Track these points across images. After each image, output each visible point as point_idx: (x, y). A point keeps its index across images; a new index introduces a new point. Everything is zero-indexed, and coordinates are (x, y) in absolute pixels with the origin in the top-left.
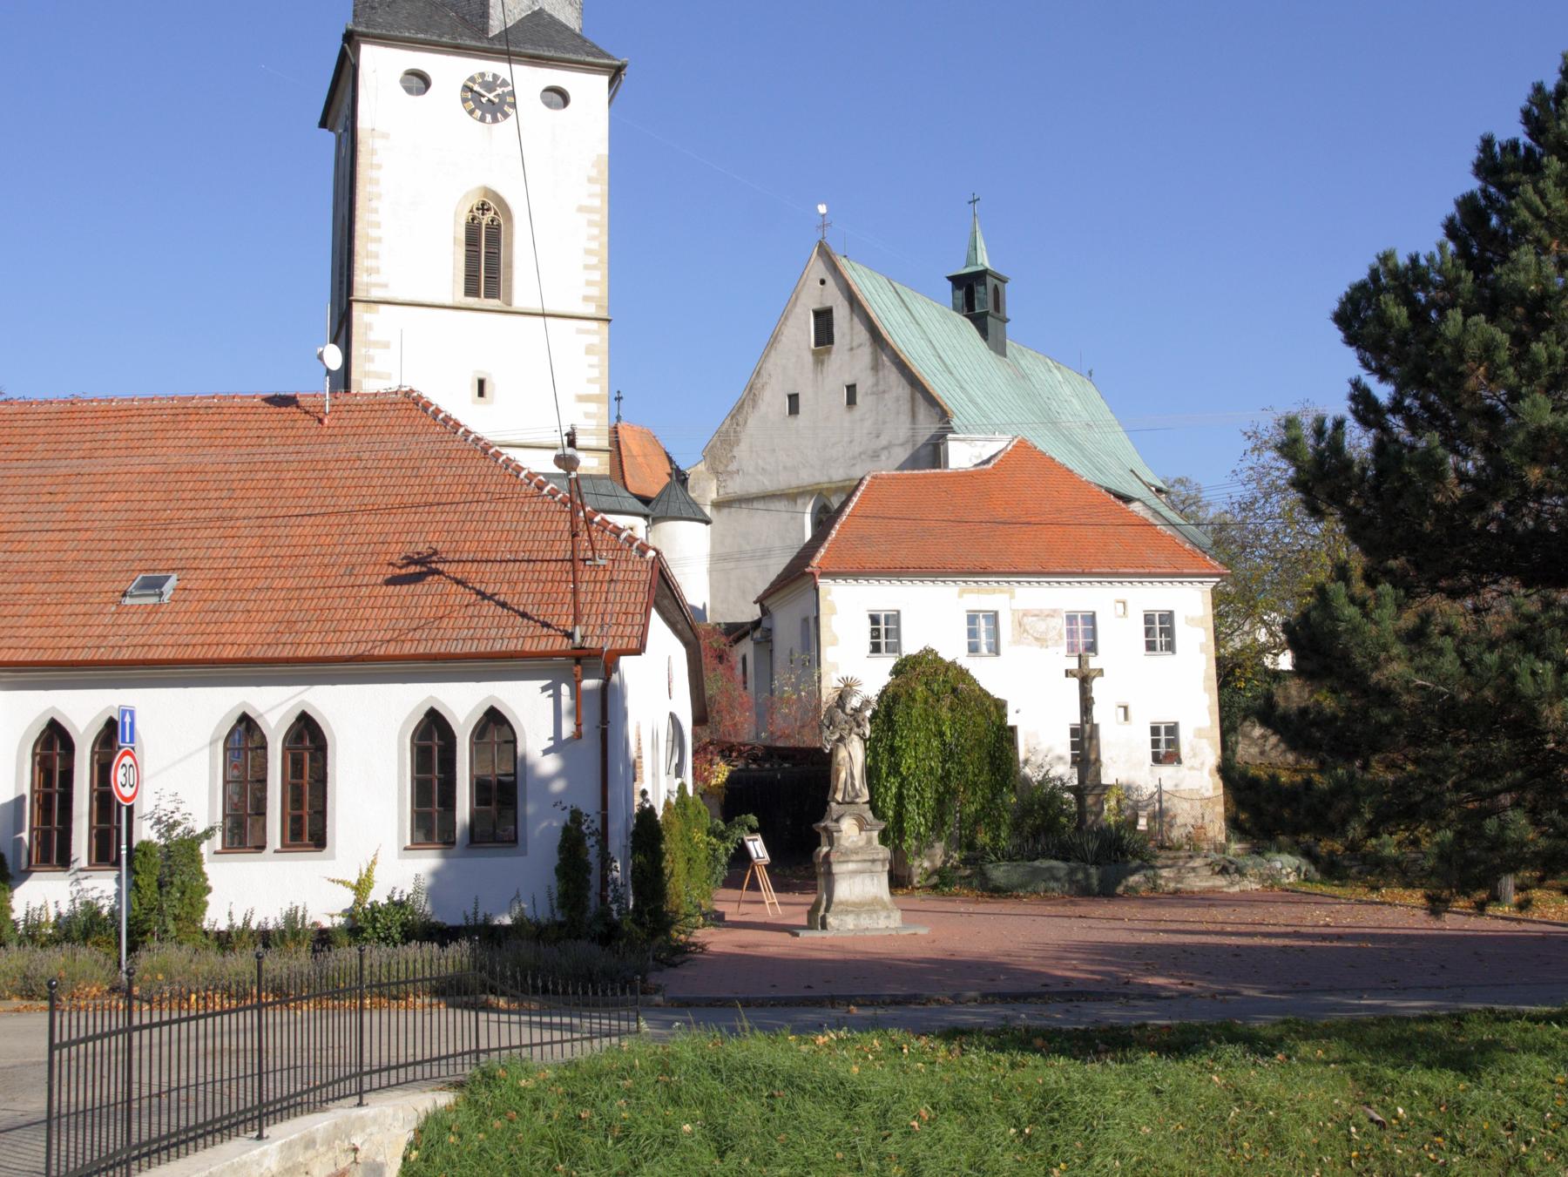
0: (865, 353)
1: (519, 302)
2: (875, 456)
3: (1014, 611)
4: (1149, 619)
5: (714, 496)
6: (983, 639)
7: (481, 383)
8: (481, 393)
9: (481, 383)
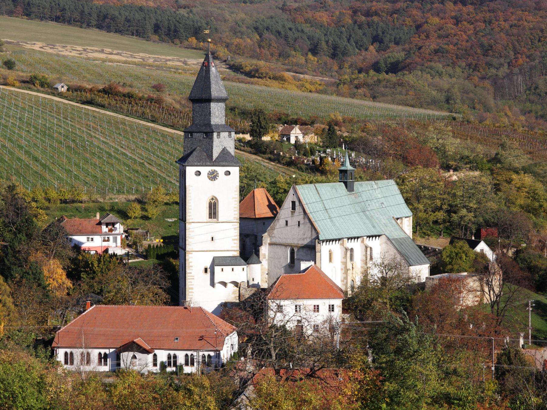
1: (220, 219)
2: (303, 240)
4: (329, 306)
5: (269, 242)
6: (298, 309)
7: (212, 238)
9: (212, 238)
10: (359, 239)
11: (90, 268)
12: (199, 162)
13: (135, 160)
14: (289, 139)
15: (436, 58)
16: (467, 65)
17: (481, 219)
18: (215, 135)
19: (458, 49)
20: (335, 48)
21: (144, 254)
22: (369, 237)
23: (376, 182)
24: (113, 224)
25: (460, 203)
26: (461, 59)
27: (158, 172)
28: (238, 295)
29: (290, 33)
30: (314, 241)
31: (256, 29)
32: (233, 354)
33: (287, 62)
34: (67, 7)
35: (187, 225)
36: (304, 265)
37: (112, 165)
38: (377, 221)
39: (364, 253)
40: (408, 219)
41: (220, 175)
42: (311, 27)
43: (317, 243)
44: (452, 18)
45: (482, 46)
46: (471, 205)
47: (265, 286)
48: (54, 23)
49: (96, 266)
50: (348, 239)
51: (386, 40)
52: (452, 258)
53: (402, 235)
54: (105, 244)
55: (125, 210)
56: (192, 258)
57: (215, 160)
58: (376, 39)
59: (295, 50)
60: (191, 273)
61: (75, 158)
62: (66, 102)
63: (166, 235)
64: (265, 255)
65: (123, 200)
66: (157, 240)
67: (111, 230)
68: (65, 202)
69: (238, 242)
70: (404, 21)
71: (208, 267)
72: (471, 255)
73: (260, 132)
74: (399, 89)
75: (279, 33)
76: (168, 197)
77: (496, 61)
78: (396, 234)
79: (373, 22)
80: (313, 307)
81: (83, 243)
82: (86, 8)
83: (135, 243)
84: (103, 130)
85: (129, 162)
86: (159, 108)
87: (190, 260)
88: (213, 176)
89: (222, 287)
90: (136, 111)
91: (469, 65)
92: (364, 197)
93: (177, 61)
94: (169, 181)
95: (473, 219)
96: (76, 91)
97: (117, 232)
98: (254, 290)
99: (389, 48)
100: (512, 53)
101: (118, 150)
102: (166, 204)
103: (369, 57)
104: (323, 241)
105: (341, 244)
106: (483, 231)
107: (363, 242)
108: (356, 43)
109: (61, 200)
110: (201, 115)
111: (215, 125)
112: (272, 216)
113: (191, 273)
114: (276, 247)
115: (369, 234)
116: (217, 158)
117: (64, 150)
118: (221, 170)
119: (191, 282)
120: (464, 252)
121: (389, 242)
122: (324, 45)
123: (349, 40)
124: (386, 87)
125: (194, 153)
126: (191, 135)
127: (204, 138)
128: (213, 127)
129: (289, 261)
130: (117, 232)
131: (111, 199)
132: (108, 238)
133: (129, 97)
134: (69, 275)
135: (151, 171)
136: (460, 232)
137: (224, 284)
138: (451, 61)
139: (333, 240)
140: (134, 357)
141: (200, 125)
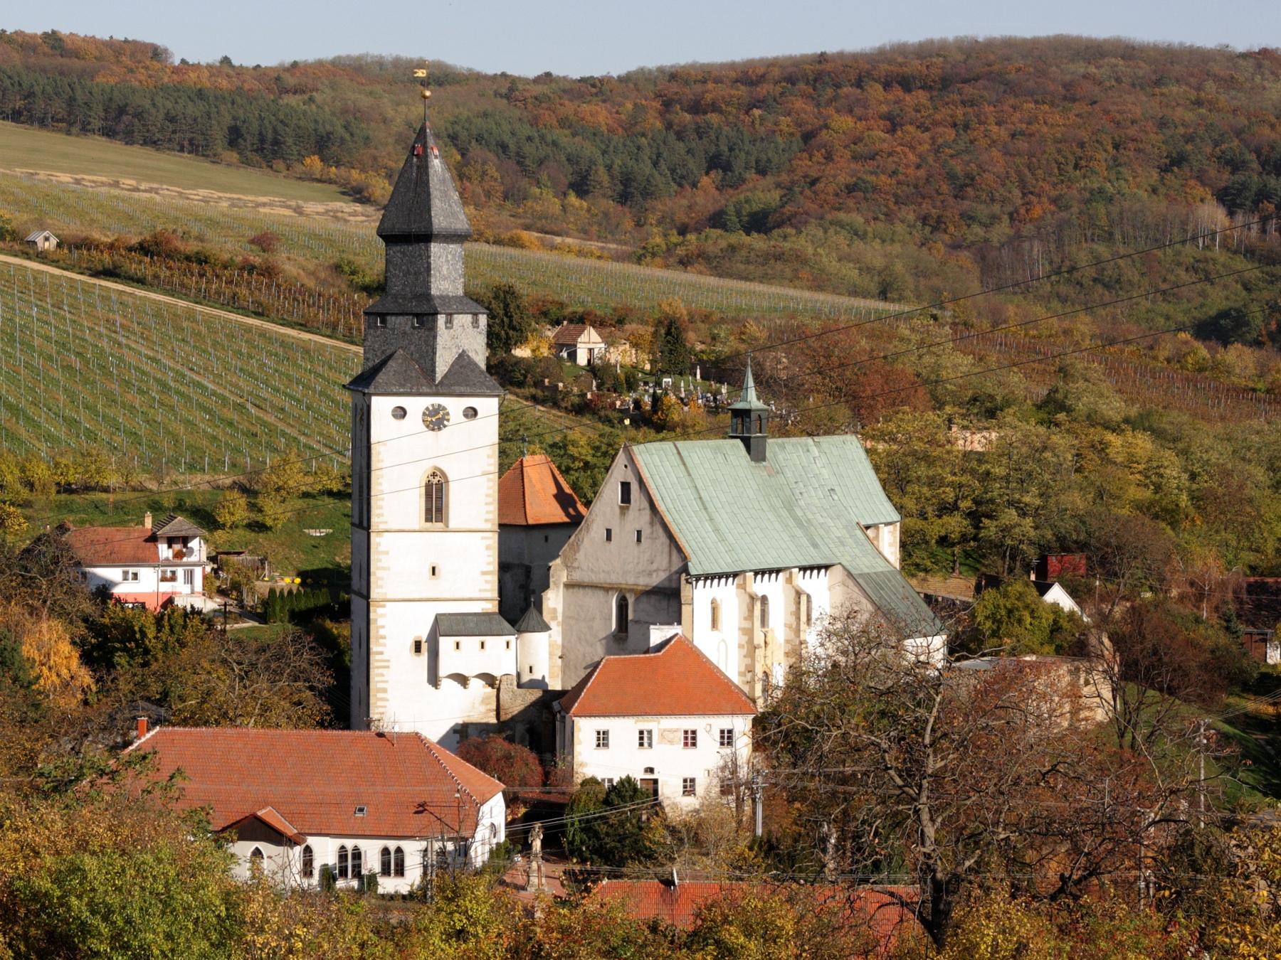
0: (647, 513)
1: (453, 523)
2: (650, 574)
3: (659, 730)
4: (722, 732)
5: (565, 579)
6: (646, 740)
7: (434, 569)
8: (434, 573)
9: (434, 569)
10: (781, 575)
11: (136, 641)
12: (403, 386)
13: (224, 399)
14: (573, 356)
15: (851, 203)
16: (918, 218)
17: (1049, 534)
18: (441, 319)
19: (899, 183)
20: (627, 180)
21: (259, 611)
22: (804, 569)
23: (816, 439)
24: (185, 540)
25: (1001, 496)
26: (906, 205)
27: (281, 426)
28: (494, 707)
29: (528, 149)
30: (675, 577)
31: (453, 138)
32: (494, 846)
33: (521, 210)
34: (37, 89)
35: (373, 536)
36: (657, 634)
37: (172, 408)
38: (821, 532)
39: (793, 608)
40: (891, 528)
41: (452, 417)
42: (574, 135)
43: (683, 582)
44: (882, 117)
45: (951, 177)
46: (1027, 499)
47: (555, 685)
48: (9, 124)
49: (150, 636)
50: (756, 573)
51: (738, 165)
52: (1000, 622)
53: (881, 567)
54: (166, 587)
55: (208, 509)
56: (384, 616)
57: (441, 382)
58: (715, 163)
59: (538, 183)
60: (381, 653)
61: (84, 393)
62: (57, 271)
63: (309, 568)
64: (555, 610)
65: (206, 487)
66: (288, 580)
67: (179, 555)
68: (67, 489)
69: (494, 579)
70: (776, 124)
71: (424, 639)
72: (1044, 615)
73: (508, 338)
74: (779, 266)
75: (504, 147)
76: (310, 479)
77: (982, 211)
78: (865, 564)
79: (709, 126)
80: (682, 735)
81: (115, 584)
82: (79, 93)
83: (236, 586)
84: (146, 332)
85: (211, 403)
86: (269, 287)
87: (380, 622)
88: (436, 420)
89: (455, 686)
90: (218, 293)
91: (925, 220)
92: (789, 474)
93: (281, 206)
94: (305, 445)
95: (1032, 533)
96: (78, 247)
97: (194, 559)
98: (536, 694)
99: (744, 181)
100: (1017, 192)
101: (184, 376)
102: (306, 495)
103: (700, 200)
104: (698, 578)
105: (739, 586)
106: (1053, 561)
107: (789, 580)
108: (673, 171)
109: (58, 484)
110: (407, 273)
111: (442, 297)
112: (566, 520)
113: (381, 653)
114: (581, 591)
115: (805, 563)
116: (445, 376)
117: (58, 375)
118: (455, 405)
119: (382, 675)
120: (1027, 607)
121: (850, 583)
122: (602, 175)
123: (655, 164)
124: (749, 263)
125: (391, 363)
126: (383, 322)
127: (414, 328)
128: (437, 302)
129: (614, 627)
130: (194, 559)
131: (176, 483)
132: (173, 573)
133: (200, 262)
134: (87, 659)
135: (264, 424)
136: (1000, 563)
137: (462, 680)
138: (884, 209)
139: (720, 576)
140: (257, 853)
141: (404, 298)
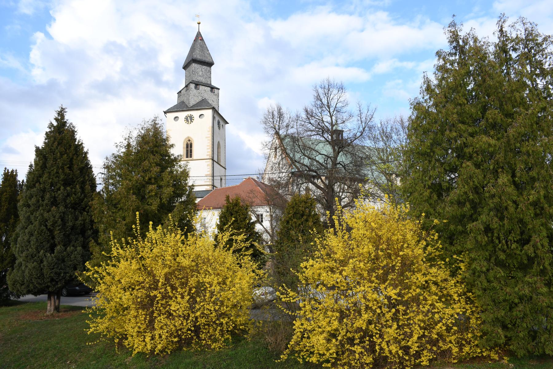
41: (195, 119)
88: (189, 119)
118: (195, 114)
